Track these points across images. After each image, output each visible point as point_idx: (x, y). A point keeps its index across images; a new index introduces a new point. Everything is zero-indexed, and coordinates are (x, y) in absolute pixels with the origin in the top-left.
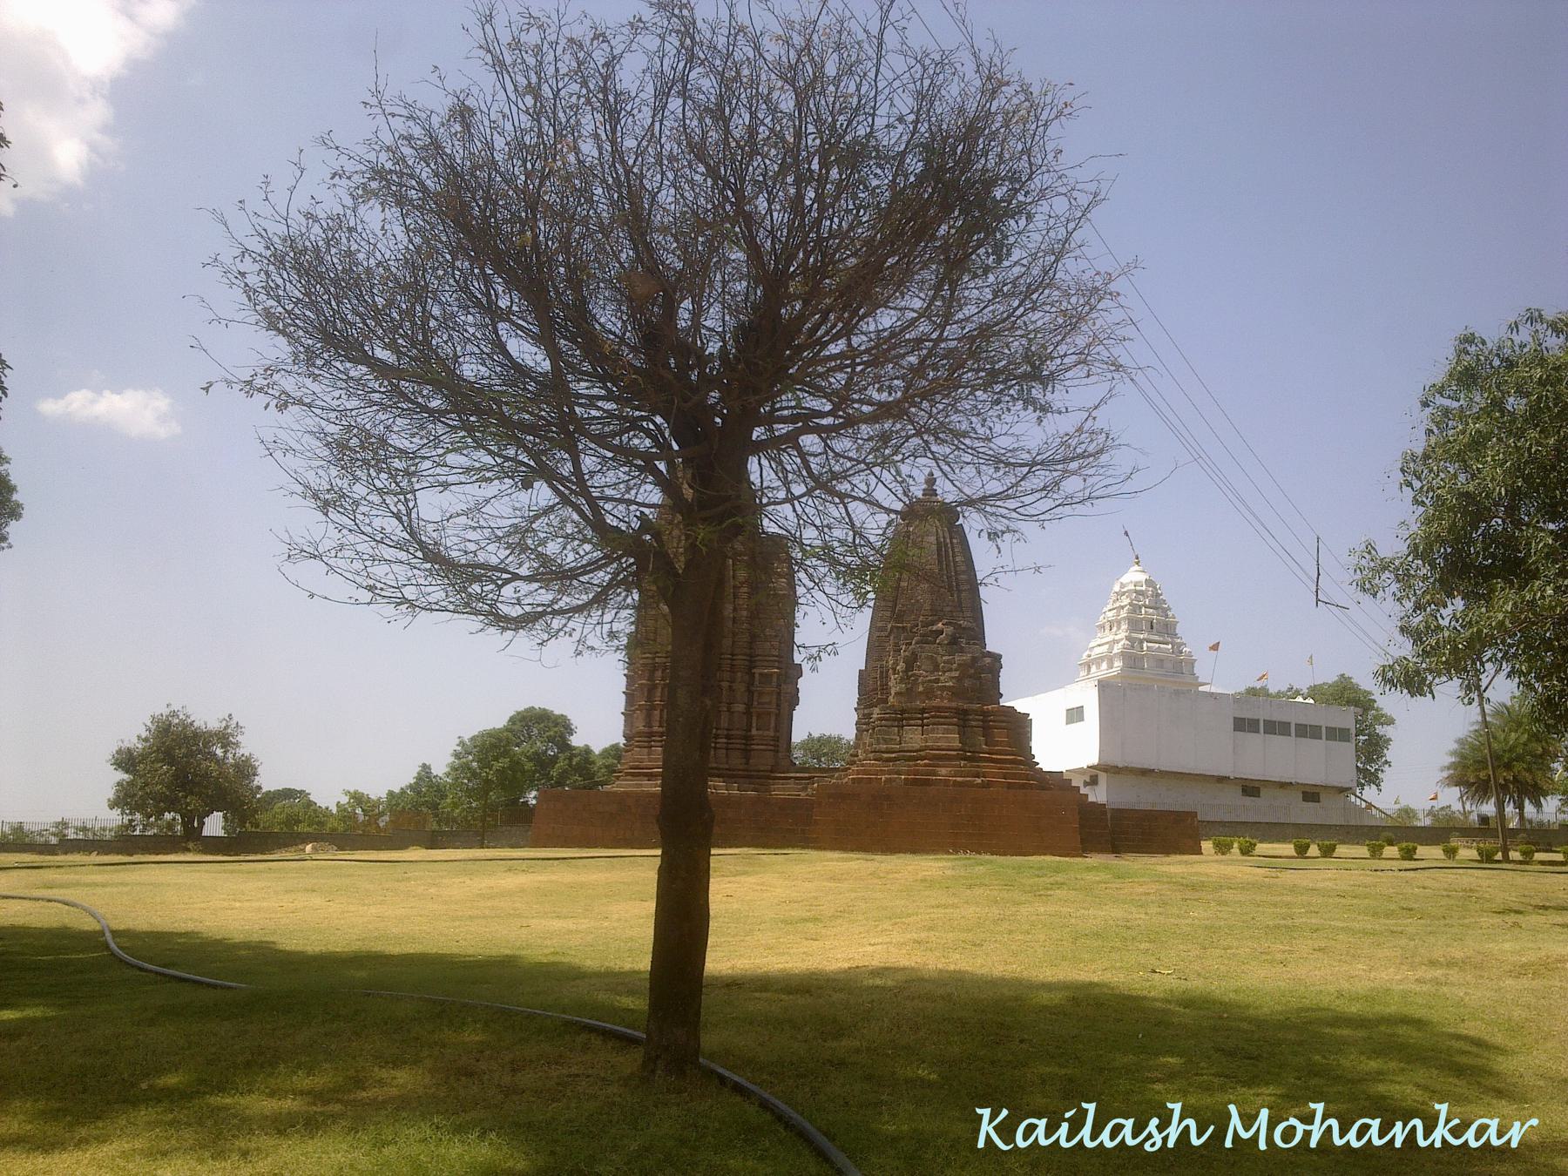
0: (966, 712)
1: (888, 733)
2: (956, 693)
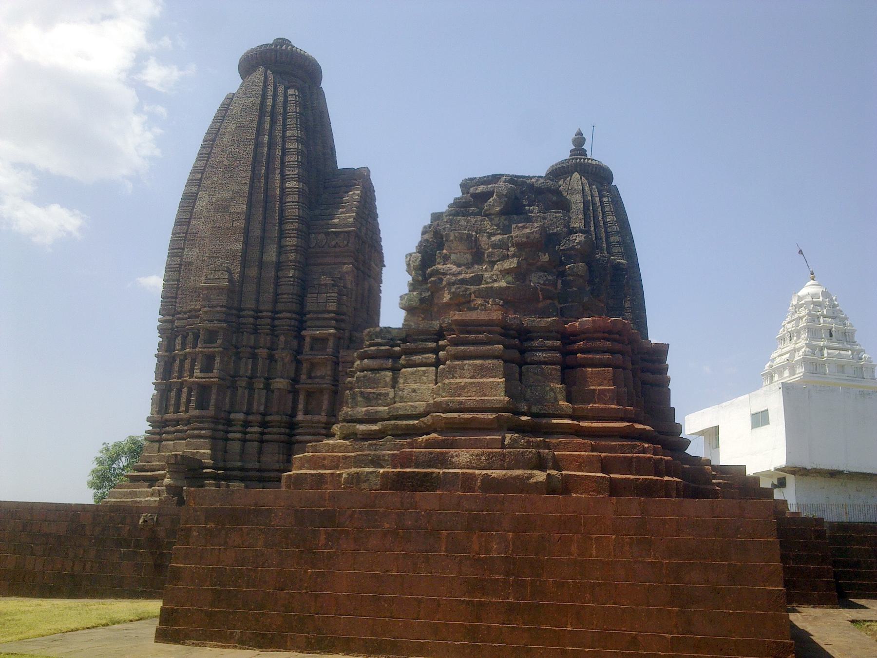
0: (524, 334)
1: (375, 383)
2: (509, 301)
